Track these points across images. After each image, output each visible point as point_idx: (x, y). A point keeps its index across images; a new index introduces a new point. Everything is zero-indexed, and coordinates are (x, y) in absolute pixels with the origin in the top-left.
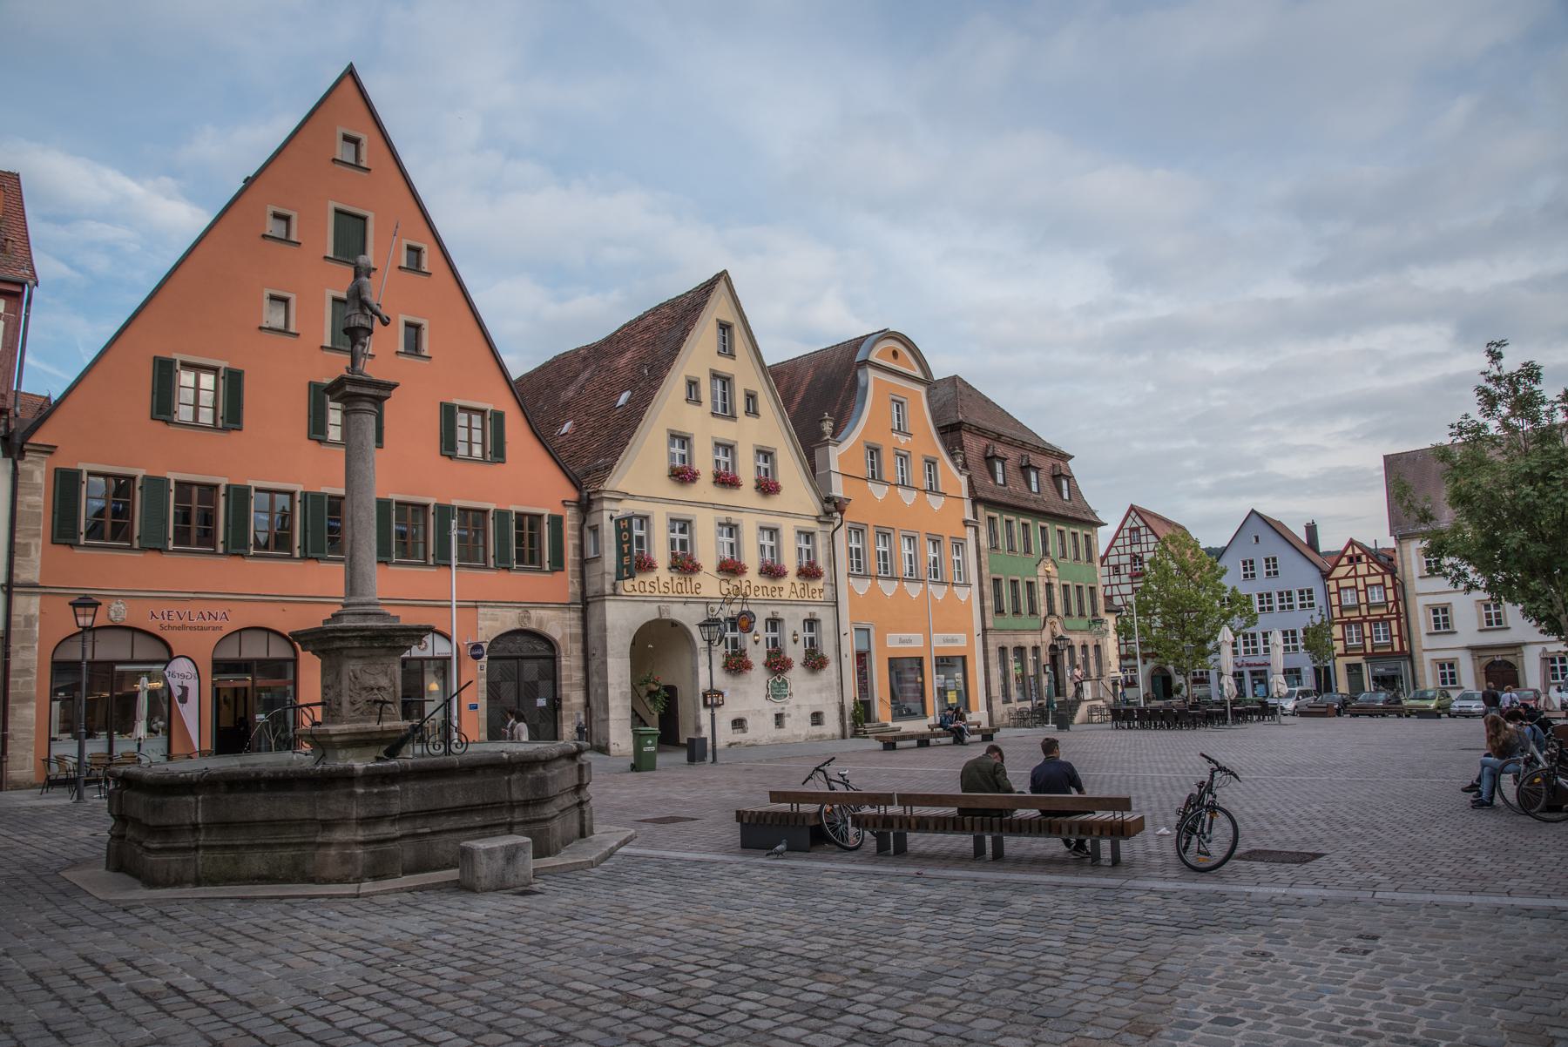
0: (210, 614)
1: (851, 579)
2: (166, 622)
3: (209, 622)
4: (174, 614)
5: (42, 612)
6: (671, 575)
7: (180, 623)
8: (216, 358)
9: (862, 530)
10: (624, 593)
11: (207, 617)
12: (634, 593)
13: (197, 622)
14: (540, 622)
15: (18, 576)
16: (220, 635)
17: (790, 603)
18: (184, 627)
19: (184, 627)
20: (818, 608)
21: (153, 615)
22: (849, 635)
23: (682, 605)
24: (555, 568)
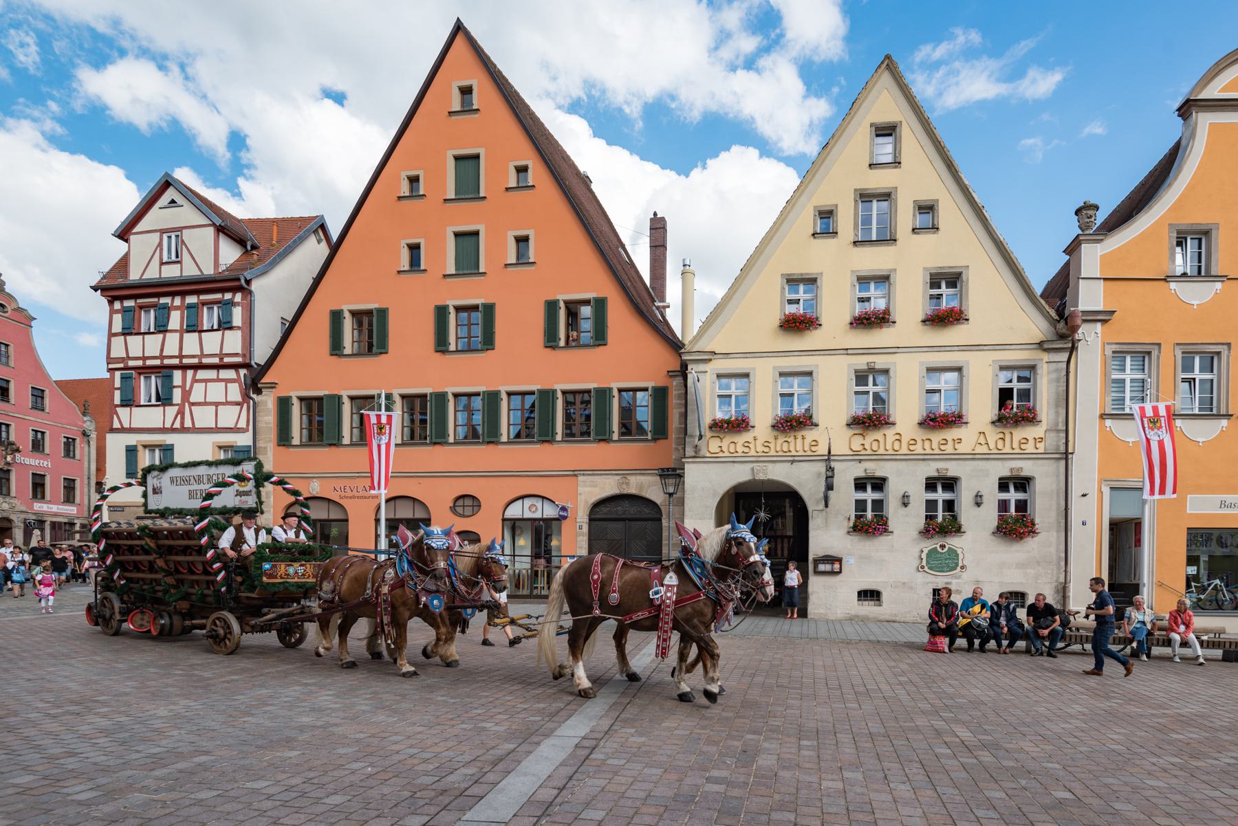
1: (1108, 423)
8: (369, 303)
9: (1149, 353)
12: (721, 454)
17: (973, 457)
20: (1030, 463)
22: (1093, 495)
24: (657, 437)
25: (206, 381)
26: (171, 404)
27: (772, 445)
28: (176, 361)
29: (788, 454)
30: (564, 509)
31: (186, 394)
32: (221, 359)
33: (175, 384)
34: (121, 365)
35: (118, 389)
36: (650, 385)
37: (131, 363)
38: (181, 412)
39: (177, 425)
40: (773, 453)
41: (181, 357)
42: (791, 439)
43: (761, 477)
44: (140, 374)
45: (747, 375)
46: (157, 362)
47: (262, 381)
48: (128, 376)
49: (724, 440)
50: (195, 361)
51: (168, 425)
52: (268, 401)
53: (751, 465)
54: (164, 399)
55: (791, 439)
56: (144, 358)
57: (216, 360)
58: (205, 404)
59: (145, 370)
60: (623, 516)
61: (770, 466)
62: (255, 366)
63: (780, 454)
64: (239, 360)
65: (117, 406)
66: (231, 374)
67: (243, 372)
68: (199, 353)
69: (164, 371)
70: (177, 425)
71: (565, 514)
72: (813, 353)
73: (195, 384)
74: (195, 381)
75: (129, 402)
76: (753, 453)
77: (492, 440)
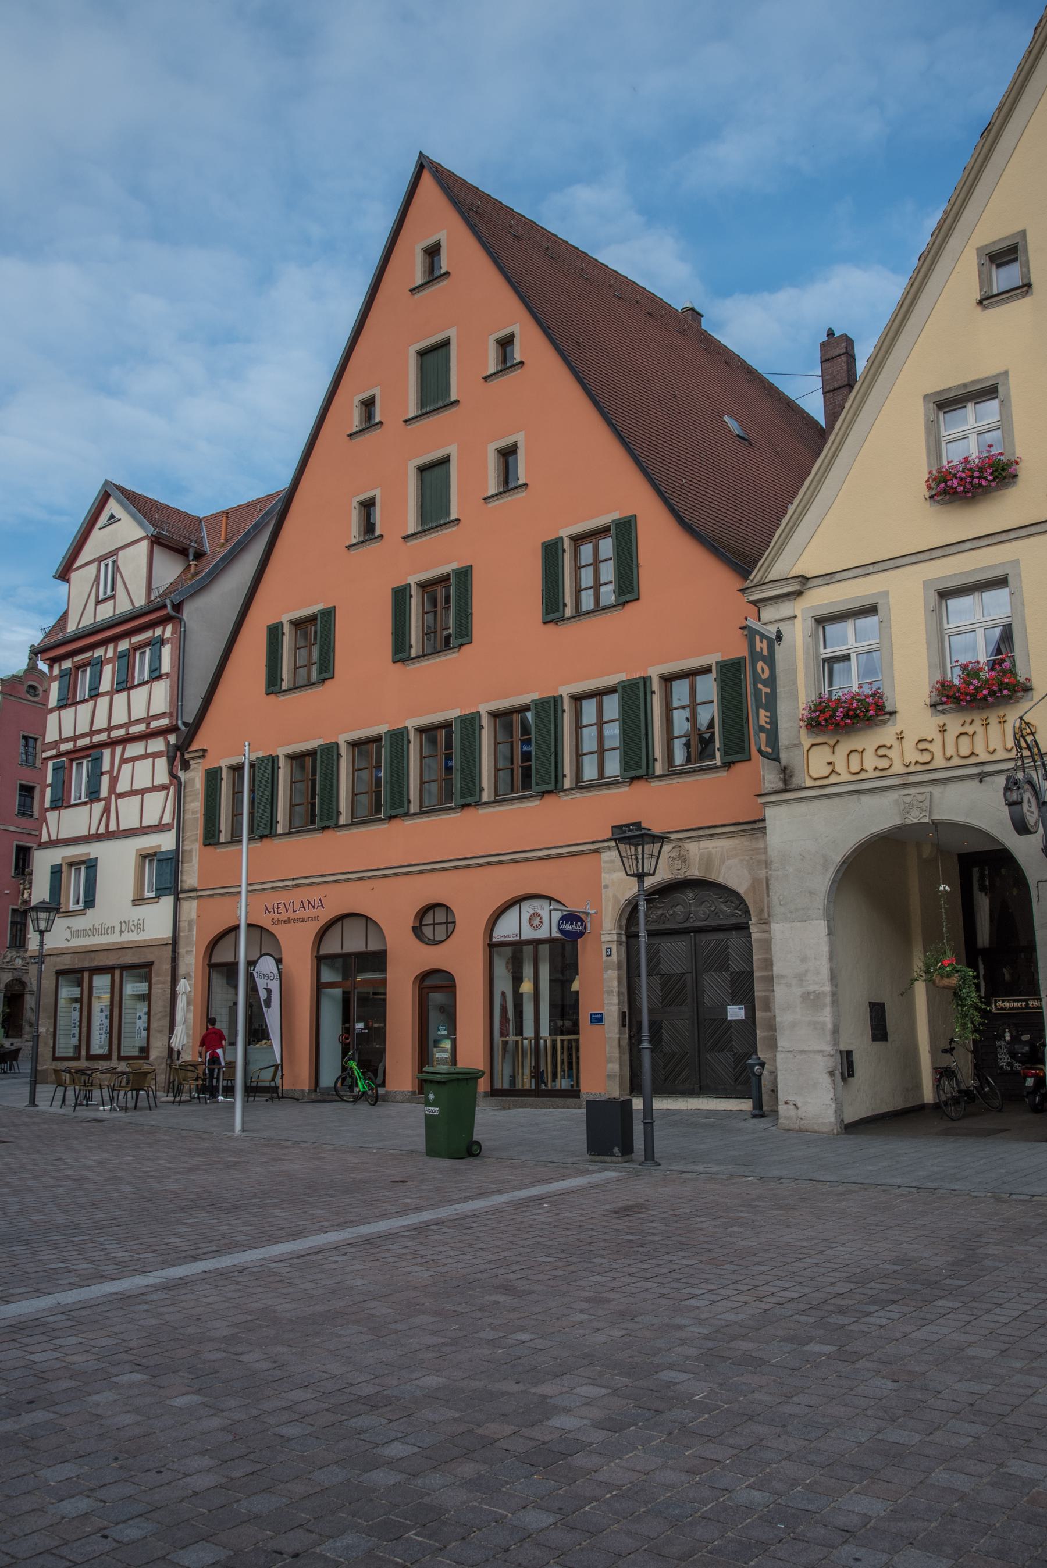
0: (309, 903)
2: (276, 916)
3: (310, 912)
4: (282, 906)
5: (198, 917)
6: (941, 719)
7: (284, 916)
10: (809, 783)
11: (306, 903)
13: (300, 913)
14: (708, 861)
15: (186, 881)
16: (314, 928)
18: (288, 921)
19: (288, 921)
21: (267, 909)
23: (975, 783)
25: (133, 759)
26: (99, 800)
27: (936, 748)
28: (103, 737)
29: (973, 760)
30: (570, 917)
31: (114, 781)
32: (148, 724)
33: (104, 770)
34: (53, 752)
35: (48, 786)
36: (712, 659)
37: (65, 747)
38: (106, 810)
39: (102, 830)
40: (939, 762)
41: (109, 729)
42: (977, 727)
43: (915, 817)
44: (72, 760)
45: (871, 610)
46: (85, 742)
47: (192, 749)
48: (61, 765)
49: (837, 749)
50: (122, 732)
51: (93, 832)
52: (195, 778)
53: (893, 795)
54: (94, 795)
55: (977, 727)
56: (75, 738)
57: (141, 728)
58: (132, 793)
59: (77, 754)
60: (687, 925)
61: (936, 791)
62: (183, 728)
63: (956, 761)
64: (165, 722)
65: (47, 810)
66: (157, 745)
67: (172, 739)
68: (126, 720)
69: (91, 752)
70: (102, 830)
71: (577, 927)
72: (1004, 537)
73: (123, 766)
74: (124, 761)
75: (60, 803)
76: (898, 768)
77: (468, 800)
